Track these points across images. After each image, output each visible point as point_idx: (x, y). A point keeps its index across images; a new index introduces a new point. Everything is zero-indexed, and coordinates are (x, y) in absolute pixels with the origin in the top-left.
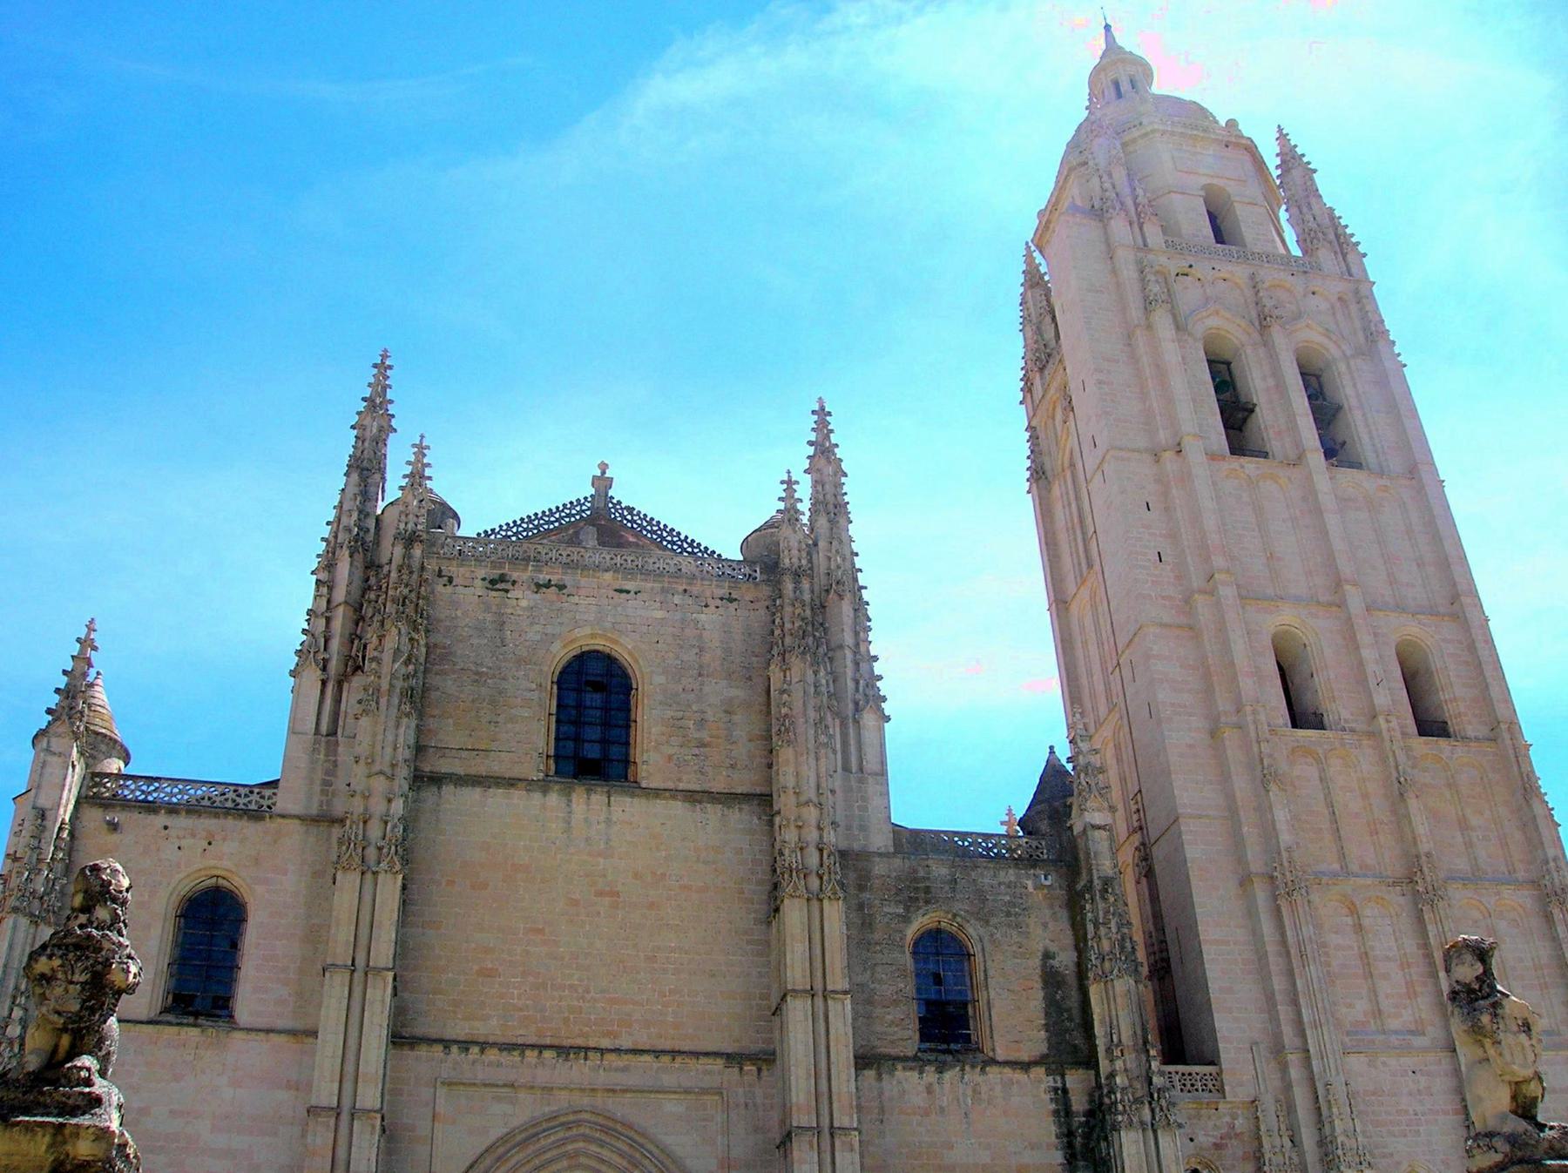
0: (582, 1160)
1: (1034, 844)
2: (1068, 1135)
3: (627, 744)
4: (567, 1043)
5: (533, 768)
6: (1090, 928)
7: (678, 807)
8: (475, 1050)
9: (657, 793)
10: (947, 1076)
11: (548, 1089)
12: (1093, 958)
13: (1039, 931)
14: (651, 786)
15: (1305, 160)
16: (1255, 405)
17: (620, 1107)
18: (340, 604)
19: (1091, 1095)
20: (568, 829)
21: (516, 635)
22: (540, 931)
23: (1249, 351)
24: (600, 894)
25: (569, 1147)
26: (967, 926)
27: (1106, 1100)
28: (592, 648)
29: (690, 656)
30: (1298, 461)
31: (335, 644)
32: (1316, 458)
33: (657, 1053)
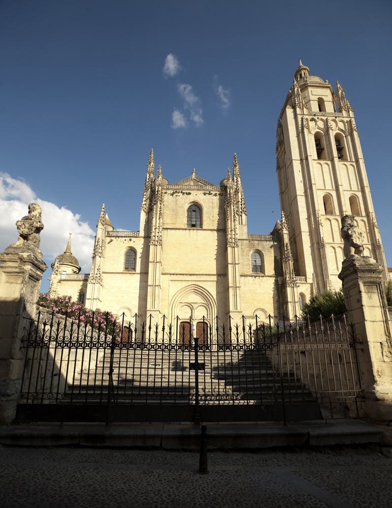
7: (209, 232)
29: (211, 205)
30: (332, 160)
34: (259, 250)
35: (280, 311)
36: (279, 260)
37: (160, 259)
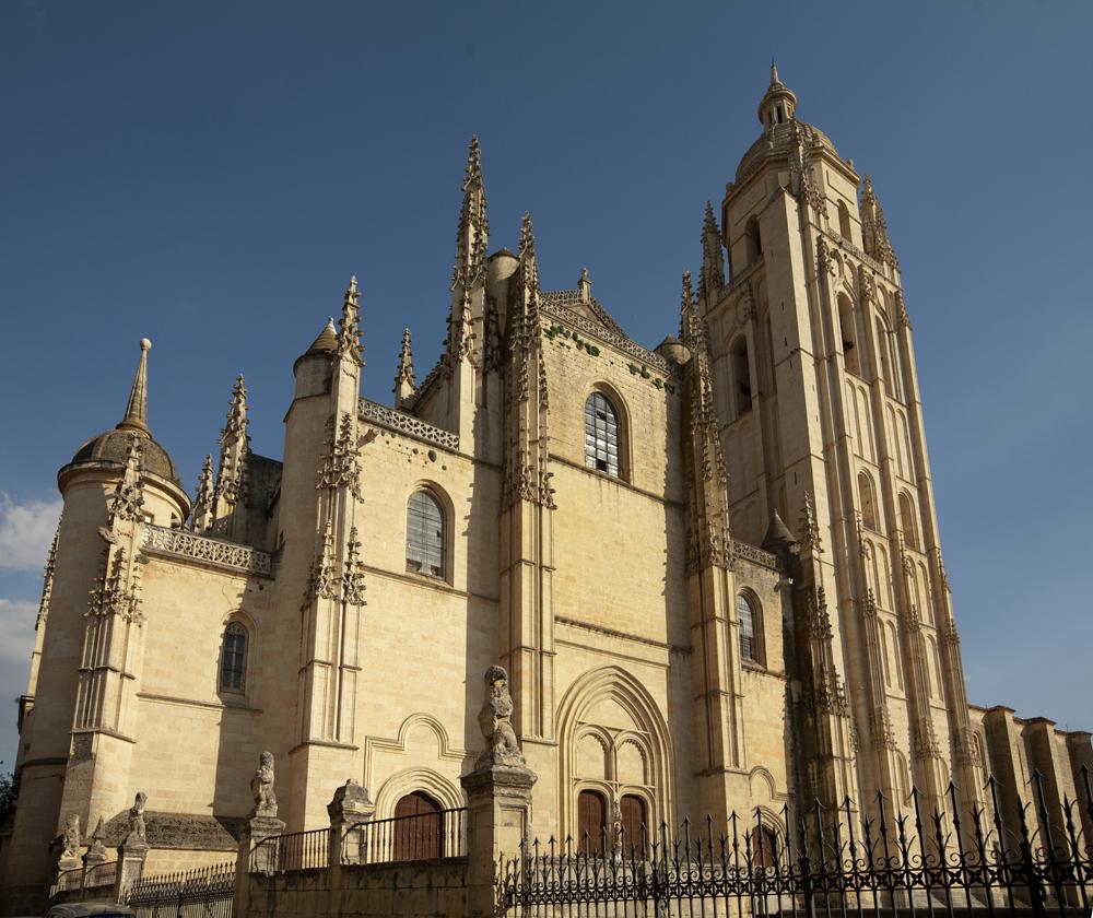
4: (608, 627)
7: (646, 500)
10: (752, 674)
11: (600, 651)
17: (628, 666)
21: (570, 370)
22: (592, 559)
24: (617, 543)
29: (647, 411)
30: (873, 384)
32: (881, 386)
33: (645, 641)
34: (752, 591)
35: (798, 780)
36: (792, 631)
37: (551, 560)
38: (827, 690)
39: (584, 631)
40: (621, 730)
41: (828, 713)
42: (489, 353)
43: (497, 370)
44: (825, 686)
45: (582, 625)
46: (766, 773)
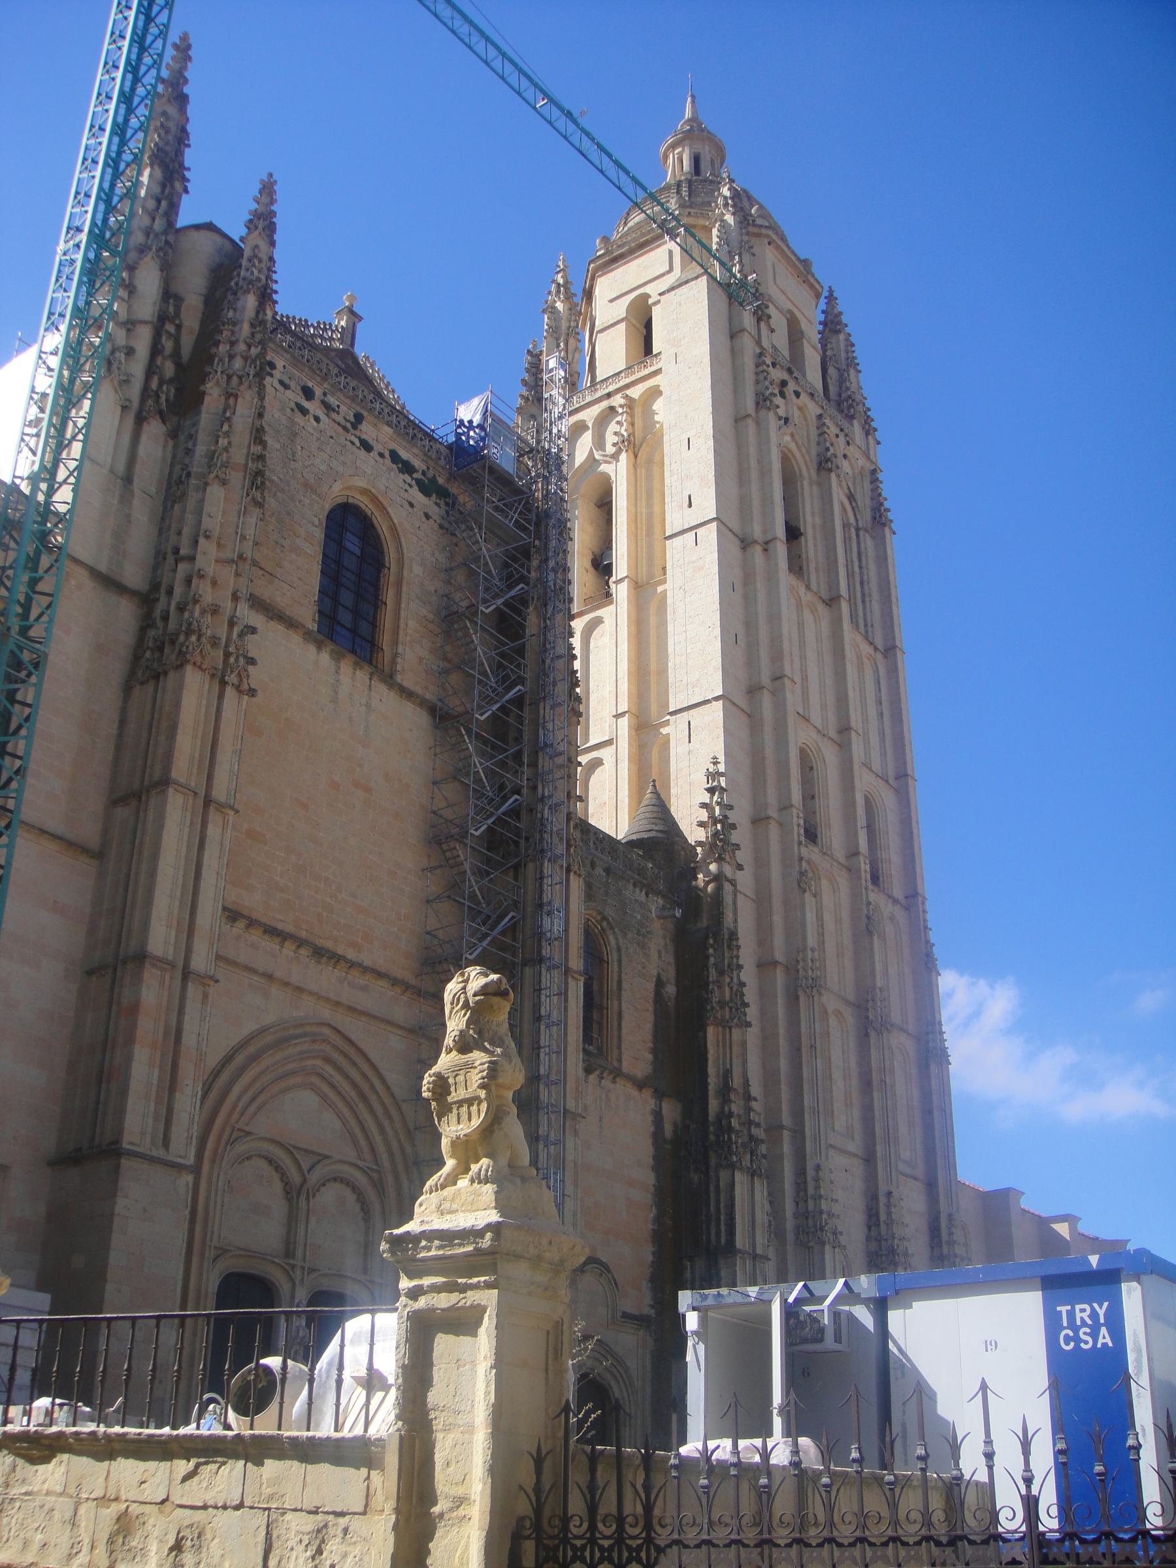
0: (315, 1080)
1: (656, 871)
2: (656, 1158)
3: (374, 625)
4: (320, 942)
5: (308, 615)
6: (713, 974)
8: (241, 924)
9: (406, 693)
10: (592, 1077)
11: (299, 990)
12: (714, 1000)
13: (656, 955)
14: (405, 684)
15: (847, 330)
16: (801, 534)
17: (355, 1028)
18: (145, 322)
19: (675, 1124)
20: (335, 700)
23: (806, 483)
25: (309, 1063)
26: (609, 932)
27: (712, 1138)
28: (356, 502)
31: (138, 368)
32: (845, 607)
34: (604, 918)
36: (671, 1004)
38: (734, 1122)
39: (269, 944)
40: (326, 1157)
41: (732, 1167)
42: (154, 385)
43: (164, 422)
44: (731, 1115)
45: (271, 931)
46: (605, 1267)
